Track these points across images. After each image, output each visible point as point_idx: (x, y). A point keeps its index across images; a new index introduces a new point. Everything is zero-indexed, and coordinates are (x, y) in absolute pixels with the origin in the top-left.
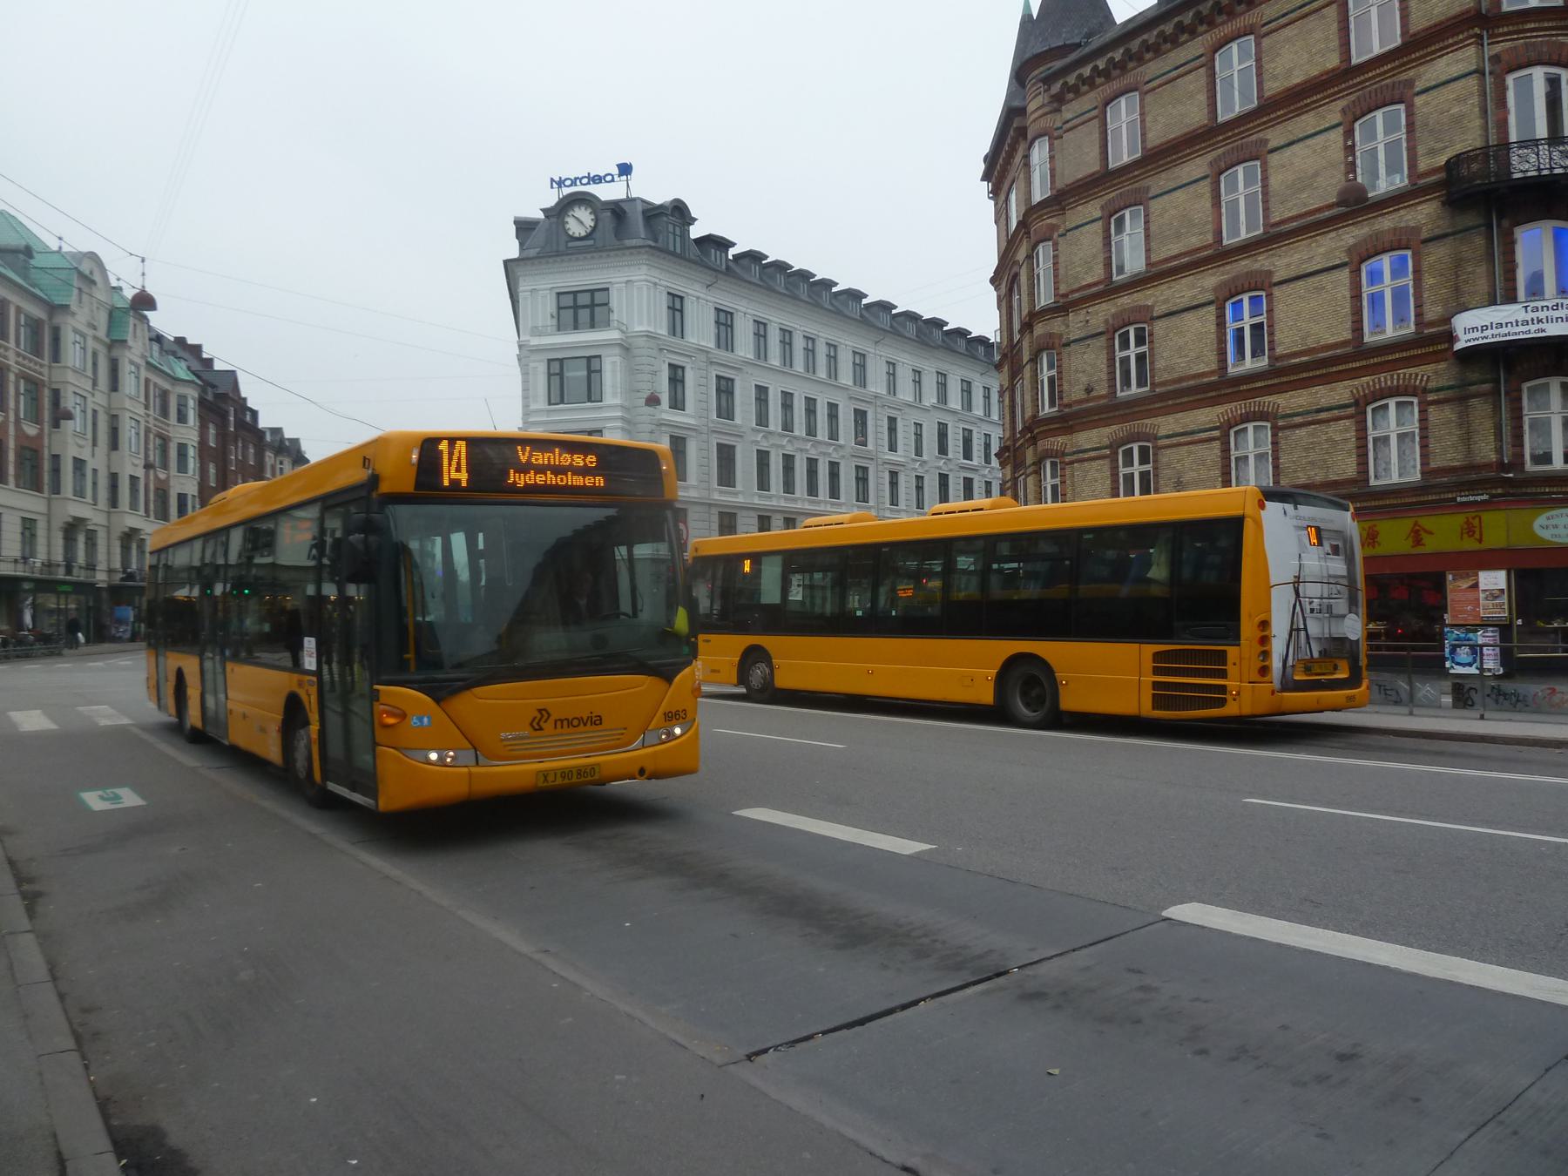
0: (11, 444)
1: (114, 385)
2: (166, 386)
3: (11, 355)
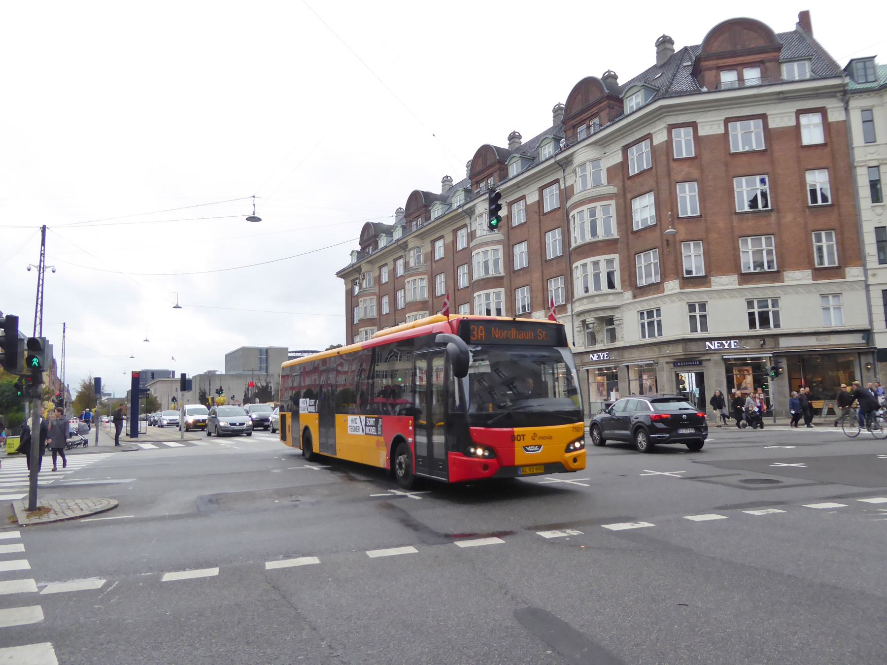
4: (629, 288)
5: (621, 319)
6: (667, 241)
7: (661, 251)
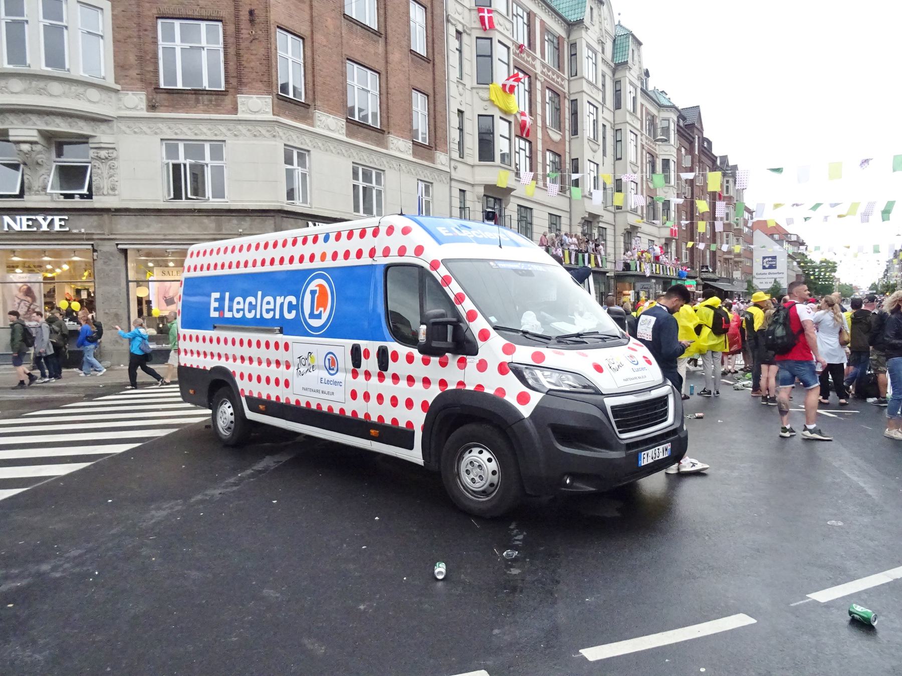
0: (540, 147)
1: (618, 105)
2: (653, 110)
3: (538, 64)
4: (139, 85)
5: (114, 149)
6: (251, 13)
7: (231, 28)
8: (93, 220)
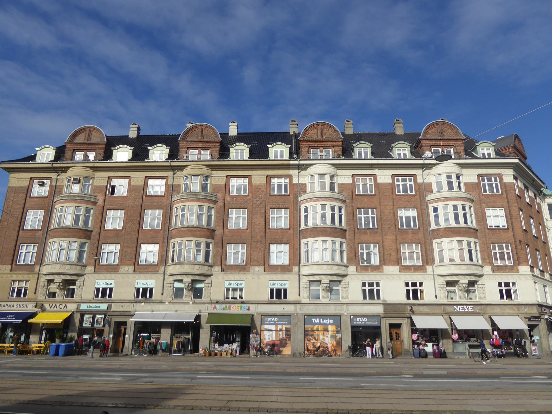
4: (489, 264)
6: (520, 241)
7: (514, 245)
8: (479, 307)
